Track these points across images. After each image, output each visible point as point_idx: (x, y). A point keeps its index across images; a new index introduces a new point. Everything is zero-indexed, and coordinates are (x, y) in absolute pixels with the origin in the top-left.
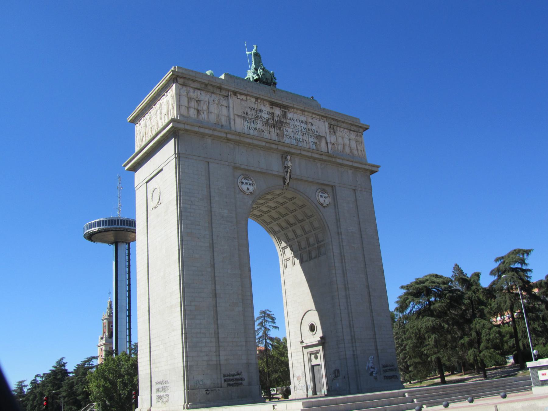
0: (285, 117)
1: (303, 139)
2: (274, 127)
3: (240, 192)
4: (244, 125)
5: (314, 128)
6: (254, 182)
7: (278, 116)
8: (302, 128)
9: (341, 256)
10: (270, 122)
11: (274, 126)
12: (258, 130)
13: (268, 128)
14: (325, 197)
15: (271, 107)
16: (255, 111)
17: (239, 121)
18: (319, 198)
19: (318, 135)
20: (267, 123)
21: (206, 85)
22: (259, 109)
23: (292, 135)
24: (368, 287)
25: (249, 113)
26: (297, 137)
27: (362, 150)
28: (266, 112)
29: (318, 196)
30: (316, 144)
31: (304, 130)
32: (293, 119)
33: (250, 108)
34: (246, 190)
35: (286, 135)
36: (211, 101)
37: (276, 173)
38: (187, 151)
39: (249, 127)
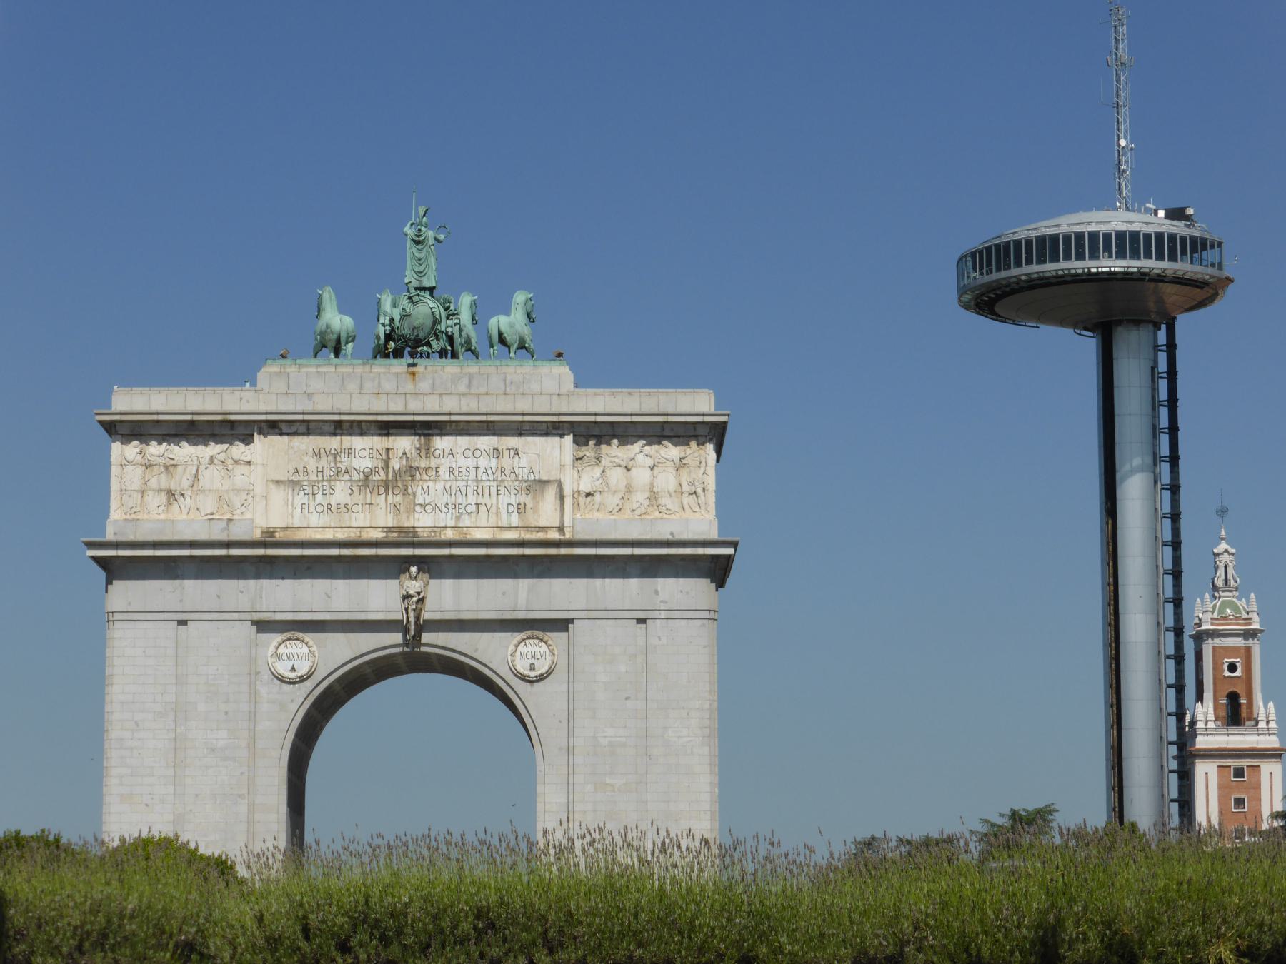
1: (477, 504)
2: (386, 491)
3: (272, 679)
4: (292, 505)
6: (314, 648)
7: (405, 454)
8: (480, 471)
10: (377, 478)
11: (386, 485)
12: (334, 509)
13: (366, 498)
16: (330, 458)
17: (278, 495)
19: (535, 480)
20: (366, 482)
22: (343, 447)
25: (312, 464)
26: (459, 501)
28: (365, 453)
31: (485, 476)
33: (317, 451)
35: (421, 505)
38: (130, 604)
39: (306, 507)
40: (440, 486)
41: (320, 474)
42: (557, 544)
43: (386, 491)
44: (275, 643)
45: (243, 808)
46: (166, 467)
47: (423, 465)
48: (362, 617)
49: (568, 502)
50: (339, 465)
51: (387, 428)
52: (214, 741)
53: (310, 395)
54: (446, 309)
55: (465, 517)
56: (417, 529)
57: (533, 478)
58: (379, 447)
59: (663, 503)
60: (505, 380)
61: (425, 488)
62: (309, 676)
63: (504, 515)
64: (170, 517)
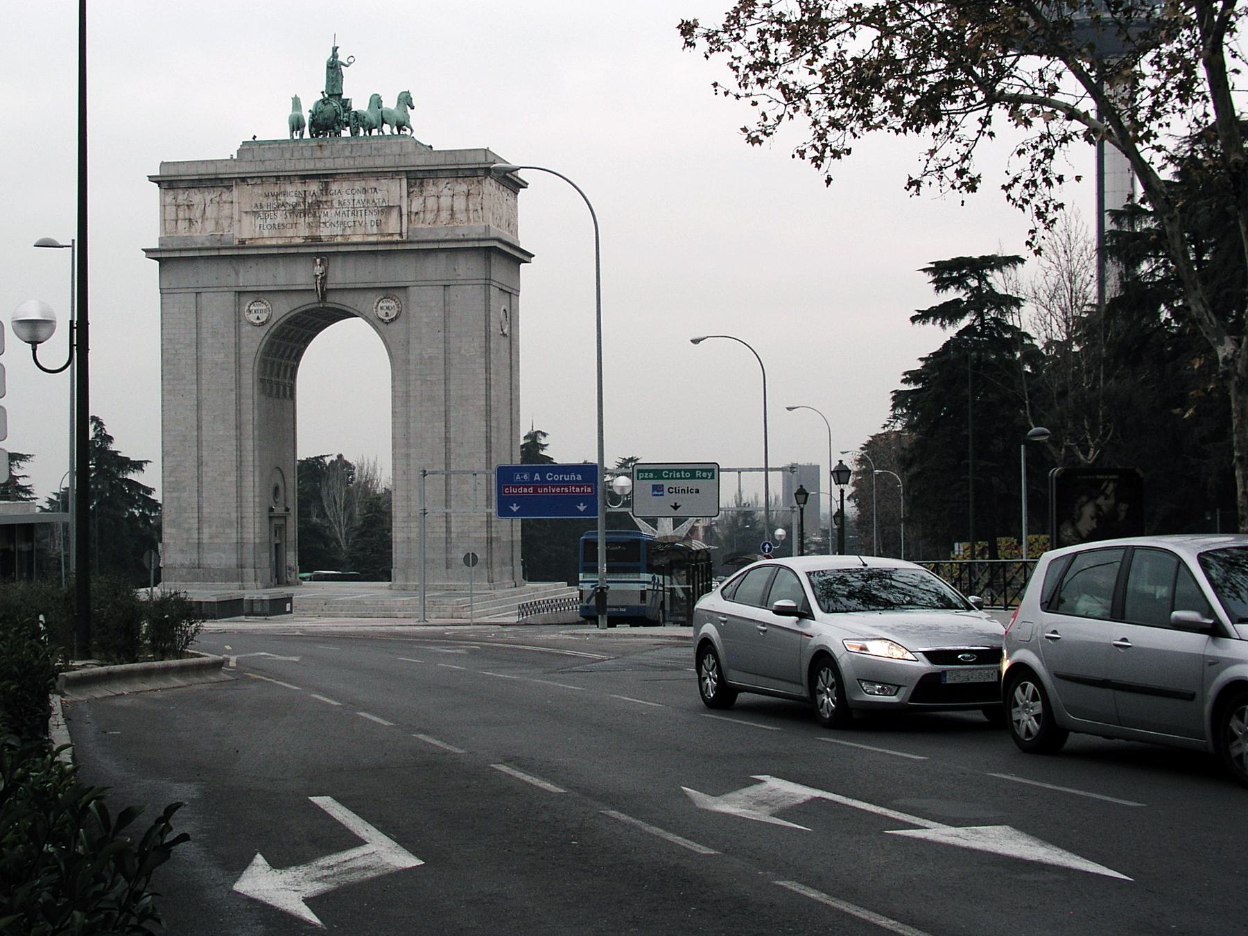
0: (326, 192)
2: (305, 216)
8: (356, 202)
10: (299, 208)
11: (305, 213)
16: (275, 198)
17: (247, 220)
20: (293, 211)
21: (200, 180)
24: (447, 440)
27: (479, 209)
28: (293, 194)
29: (376, 308)
32: (339, 191)
36: (208, 202)
40: (333, 211)
42: (397, 243)
43: (305, 216)
44: (248, 304)
46: (188, 206)
47: (324, 200)
51: (305, 178)
53: (263, 162)
54: (344, 107)
57: (384, 205)
62: (267, 321)
63: (369, 227)
64: (191, 234)
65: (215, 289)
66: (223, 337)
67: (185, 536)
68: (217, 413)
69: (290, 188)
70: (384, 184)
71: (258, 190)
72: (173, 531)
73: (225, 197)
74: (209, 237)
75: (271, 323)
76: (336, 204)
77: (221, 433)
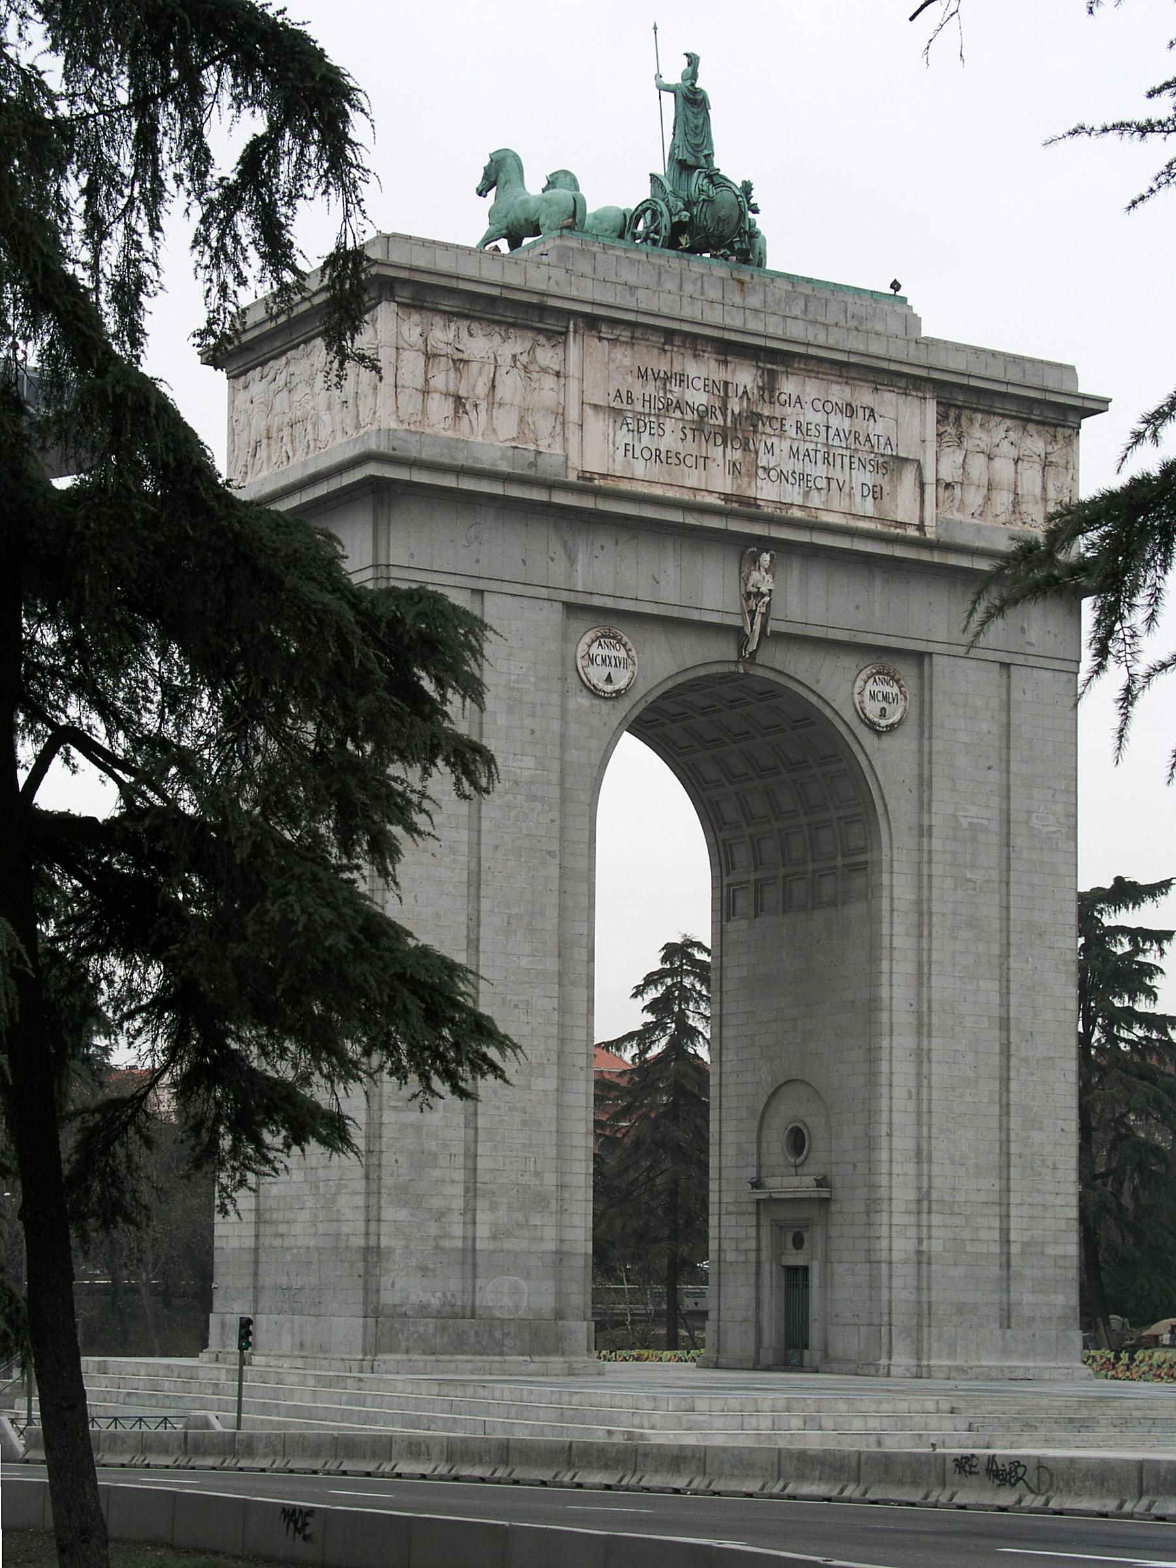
0: (771, 396)
2: (725, 443)
5: (878, 428)
7: (745, 392)
8: (832, 432)
9: (920, 914)
10: (712, 422)
11: (725, 436)
12: (663, 456)
14: (885, 698)
15: (722, 358)
16: (659, 383)
17: (597, 425)
18: (861, 702)
23: (787, 468)
24: (1005, 1024)
28: (699, 384)
30: (878, 495)
33: (643, 371)
34: (602, 685)
35: (764, 468)
37: (714, 618)
38: (412, 556)
39: (630, 448)
40: (785, 445)
41: (647, 404)
44: (587, 639)
45: (554, 871)
47: (766, 413)
48: (695, 616)
49: (930, 491)
50: (669, 396)
52: (519, 771)
55: (814, 493)
56: (759, 502)
58: (714, 376)
59: (1030, 511)
60: (846, 312)
61: (769, 445)
62: (627, 690)
65: (518, 589)
66: (533, 715)
67: (433, 1229)
68: (515, 911)
69: (693, 369)
70: (888, 402)
71: (623, 357)
72: (403, 1215)
73: (547, 356)
74: (510, 453)
75: (637, 695)
76: (791, 432)
77: (524, 962)
